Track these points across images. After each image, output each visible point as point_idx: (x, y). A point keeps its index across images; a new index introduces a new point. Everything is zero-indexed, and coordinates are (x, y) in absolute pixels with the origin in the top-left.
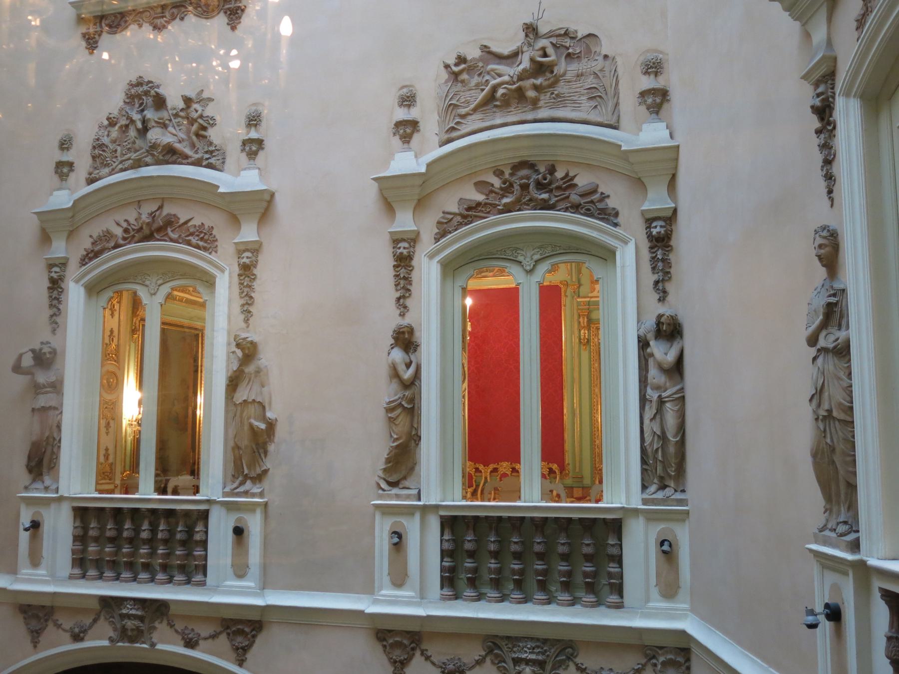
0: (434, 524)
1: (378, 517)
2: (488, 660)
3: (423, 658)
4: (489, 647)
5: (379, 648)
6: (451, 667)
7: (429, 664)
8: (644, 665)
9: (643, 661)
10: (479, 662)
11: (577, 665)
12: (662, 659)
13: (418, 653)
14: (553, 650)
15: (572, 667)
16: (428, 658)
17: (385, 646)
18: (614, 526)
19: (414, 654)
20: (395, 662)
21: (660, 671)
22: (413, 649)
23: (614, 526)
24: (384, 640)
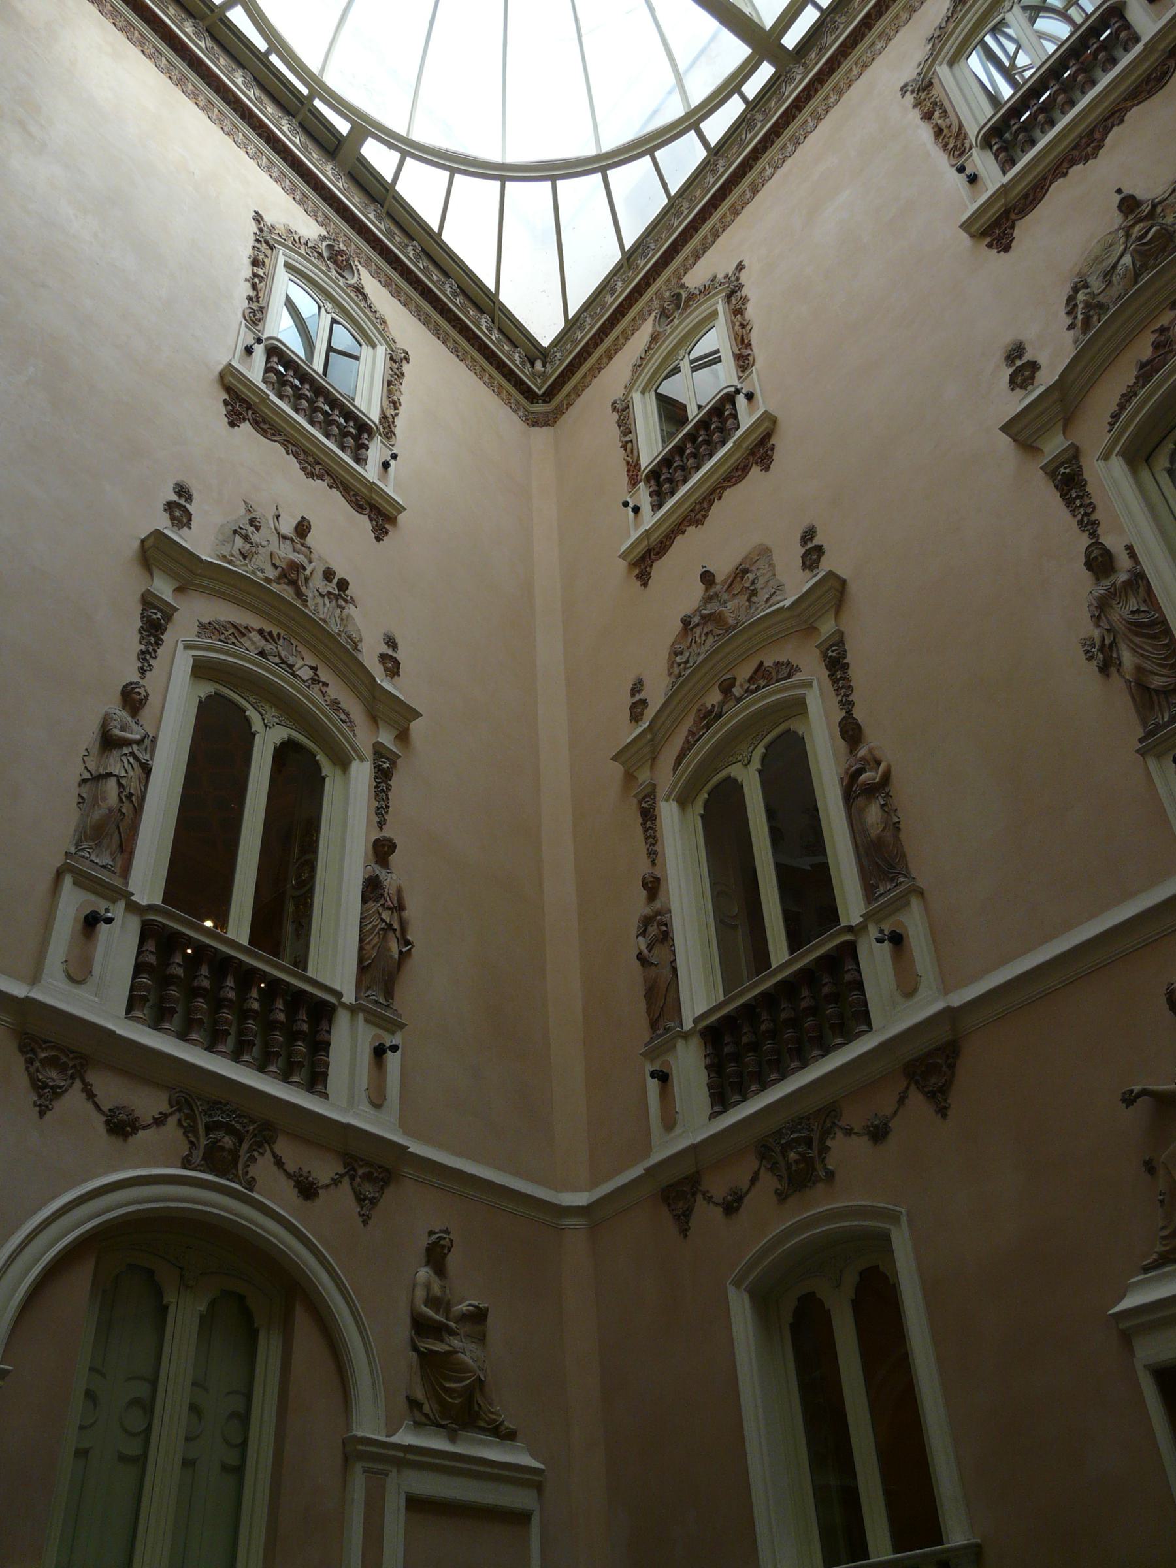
0: (133, 926)
1: (68, 880)
2: (172, 1121)
3: (84, 1095)
4: (178, 1103)
5: (19, 1062)
6: (122, 1116)
7: (89, 1106)
8: (342, 1176)
9: (341, 1170)
10: (159, 1121)
11: (274, 1155)
12: (360, 1172)
13: (78, 1085)
14: (251, 1128)
16: (90, 1095)
17: (30, 1062)
18: (320, 1011)
19: (70, 1086)
20: (46, 1086)
22: (72, 1077)
23: (320, 1011)
24: (33, 1051)
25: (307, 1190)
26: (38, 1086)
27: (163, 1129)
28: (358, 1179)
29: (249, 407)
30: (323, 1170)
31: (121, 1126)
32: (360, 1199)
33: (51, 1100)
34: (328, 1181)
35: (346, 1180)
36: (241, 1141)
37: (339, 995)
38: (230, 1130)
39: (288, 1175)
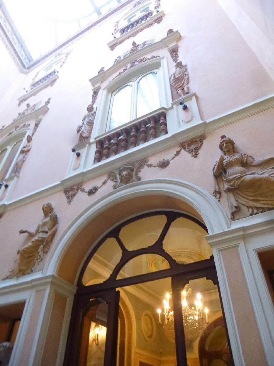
8: (180, 151)
9: (178, 149)
15: (146, 167)
19: (77, 192)
21: (188, 148)
22: (78, 190)
25: (164, 165)
26: (68, 198)
27: (106, 185)
28: (187, 147)
29: (116, 44)
30: (167, 156)
31: (91, 192)
32: (190, 152)
33: (72, 199)
34: (174, 156)
35: (183, 151)
36: (132, 170)
37: (165, 109)
38: (124, 169)
39: (155, 167)
